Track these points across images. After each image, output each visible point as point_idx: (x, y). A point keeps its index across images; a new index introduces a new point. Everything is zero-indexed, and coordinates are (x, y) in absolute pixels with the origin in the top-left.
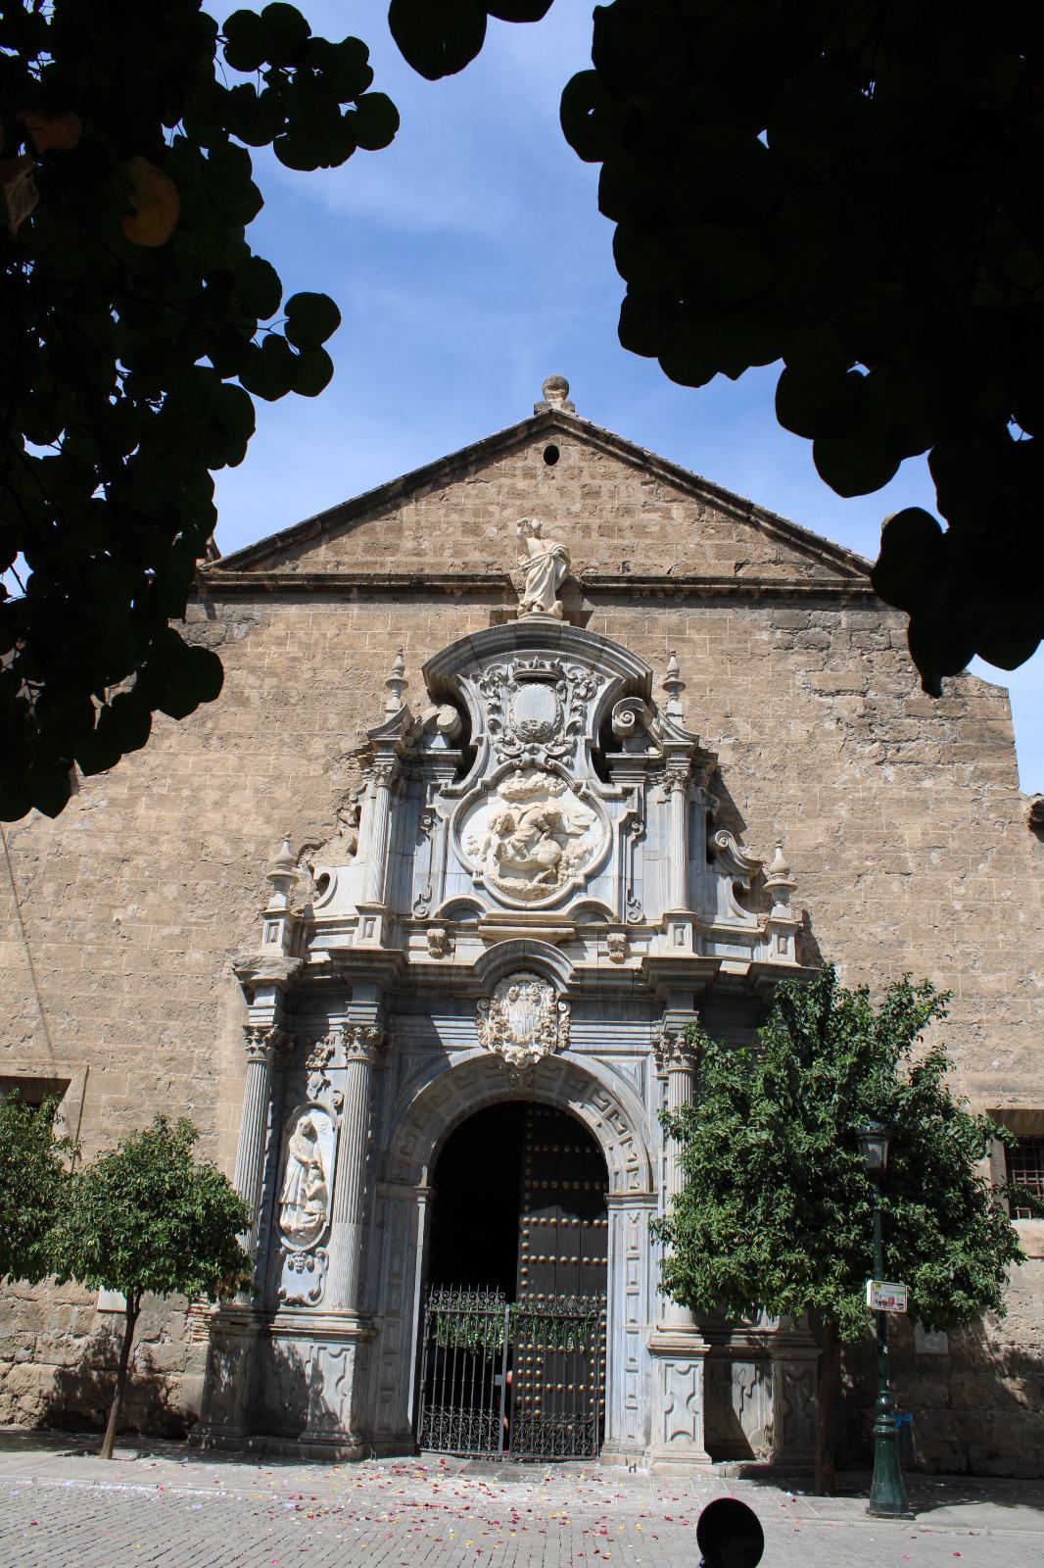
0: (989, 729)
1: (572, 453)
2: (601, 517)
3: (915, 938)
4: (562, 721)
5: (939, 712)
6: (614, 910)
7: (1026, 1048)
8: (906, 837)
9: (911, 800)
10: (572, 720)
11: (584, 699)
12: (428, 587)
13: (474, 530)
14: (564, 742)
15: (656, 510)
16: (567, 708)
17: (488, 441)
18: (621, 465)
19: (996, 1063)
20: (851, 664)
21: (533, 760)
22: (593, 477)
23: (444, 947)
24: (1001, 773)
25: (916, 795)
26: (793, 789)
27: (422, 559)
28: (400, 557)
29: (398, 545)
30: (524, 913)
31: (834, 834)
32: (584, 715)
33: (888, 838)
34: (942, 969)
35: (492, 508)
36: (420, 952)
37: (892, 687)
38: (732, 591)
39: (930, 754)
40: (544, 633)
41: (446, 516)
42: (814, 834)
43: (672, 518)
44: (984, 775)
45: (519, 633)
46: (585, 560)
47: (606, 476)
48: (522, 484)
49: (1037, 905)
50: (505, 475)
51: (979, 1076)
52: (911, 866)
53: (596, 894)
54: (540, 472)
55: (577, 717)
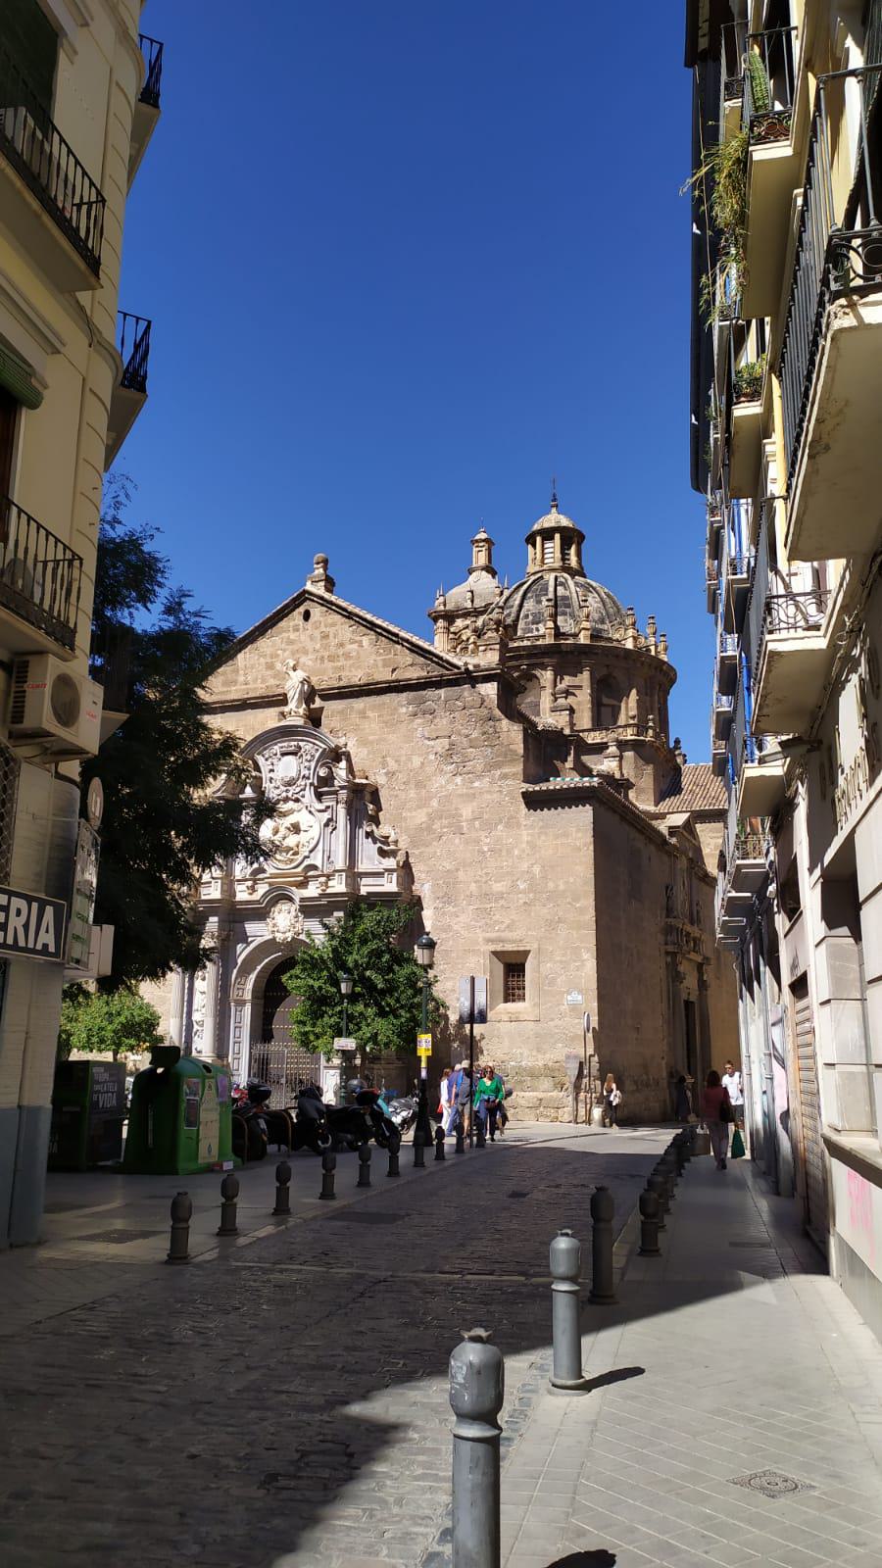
0: (511, 750)
1: (317, 611)
3: (464, 867)
4: (299, 774)
6: (320, 866)
7: (512, 920)
8: (464, 815)
9: (467, 795)
11: (310, 761)
13: (270, 666)
16: (302, 766)
18: (340, 616)
20: (444, 721)
22: (326, 627)
23: (253, 889)
24: (514, 775)
25: (471, 791)
26: (412, 794)
28: (238, 687)
31: (429, 815)
32: (309, 769)
33: (457, 816)
34: (475, 882)
35: (279, 652)
36: (242, 894)
37: (463, 731)
39: (480, 768)
41: (258, 659)
42: (420, 817)
44: (504, 777)
47: (333, 625)
48: (293, 636)
49: (524, 845)
50: (285, 631)
51: (488, 935)
52: (465, 830)
53: (315, 858)
54: (301, 627)
55: (307, 772)
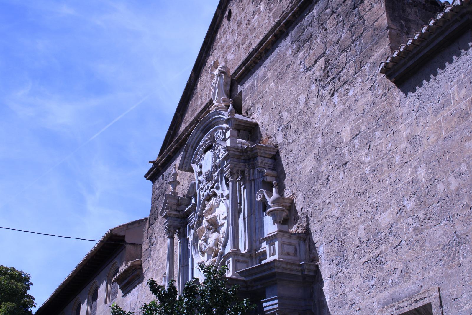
5: (354, 38)
17: (210, 29)
19: (390, 282)
38: (275, 35)
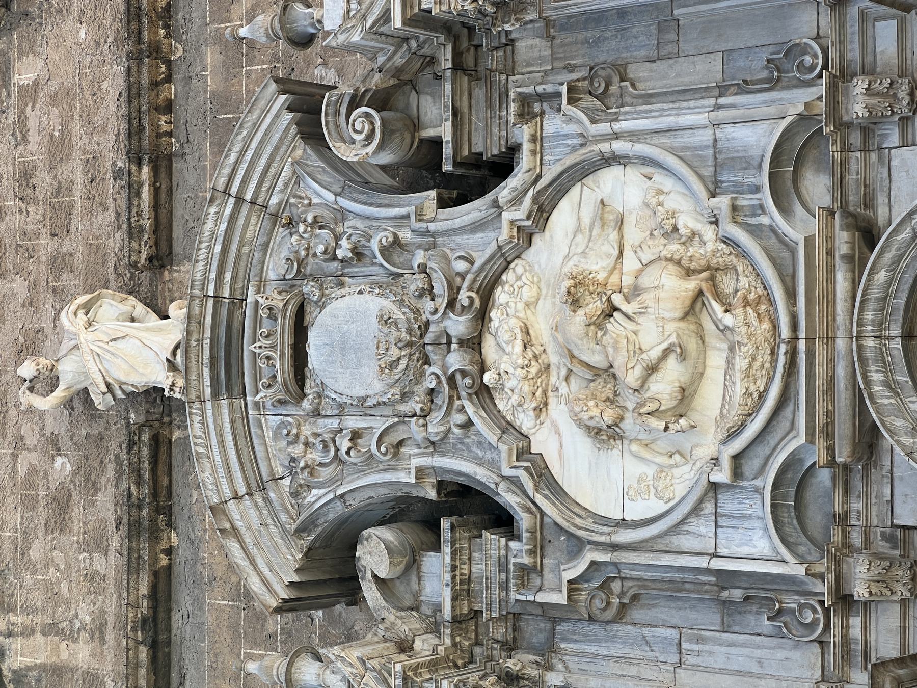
2: (37, 235)
10: (380, 259)
12: (154, 608)
14: (423, 269)
15: (22, 119)
21: (461, 343)
27: (111, 619)
29: (86, 673)
30: (802, 345)
35: (22, 471)
40: (208, 334)
41: (34, 573)
43: (36, 83)
45: (208, 391)
46: (111, 264)
